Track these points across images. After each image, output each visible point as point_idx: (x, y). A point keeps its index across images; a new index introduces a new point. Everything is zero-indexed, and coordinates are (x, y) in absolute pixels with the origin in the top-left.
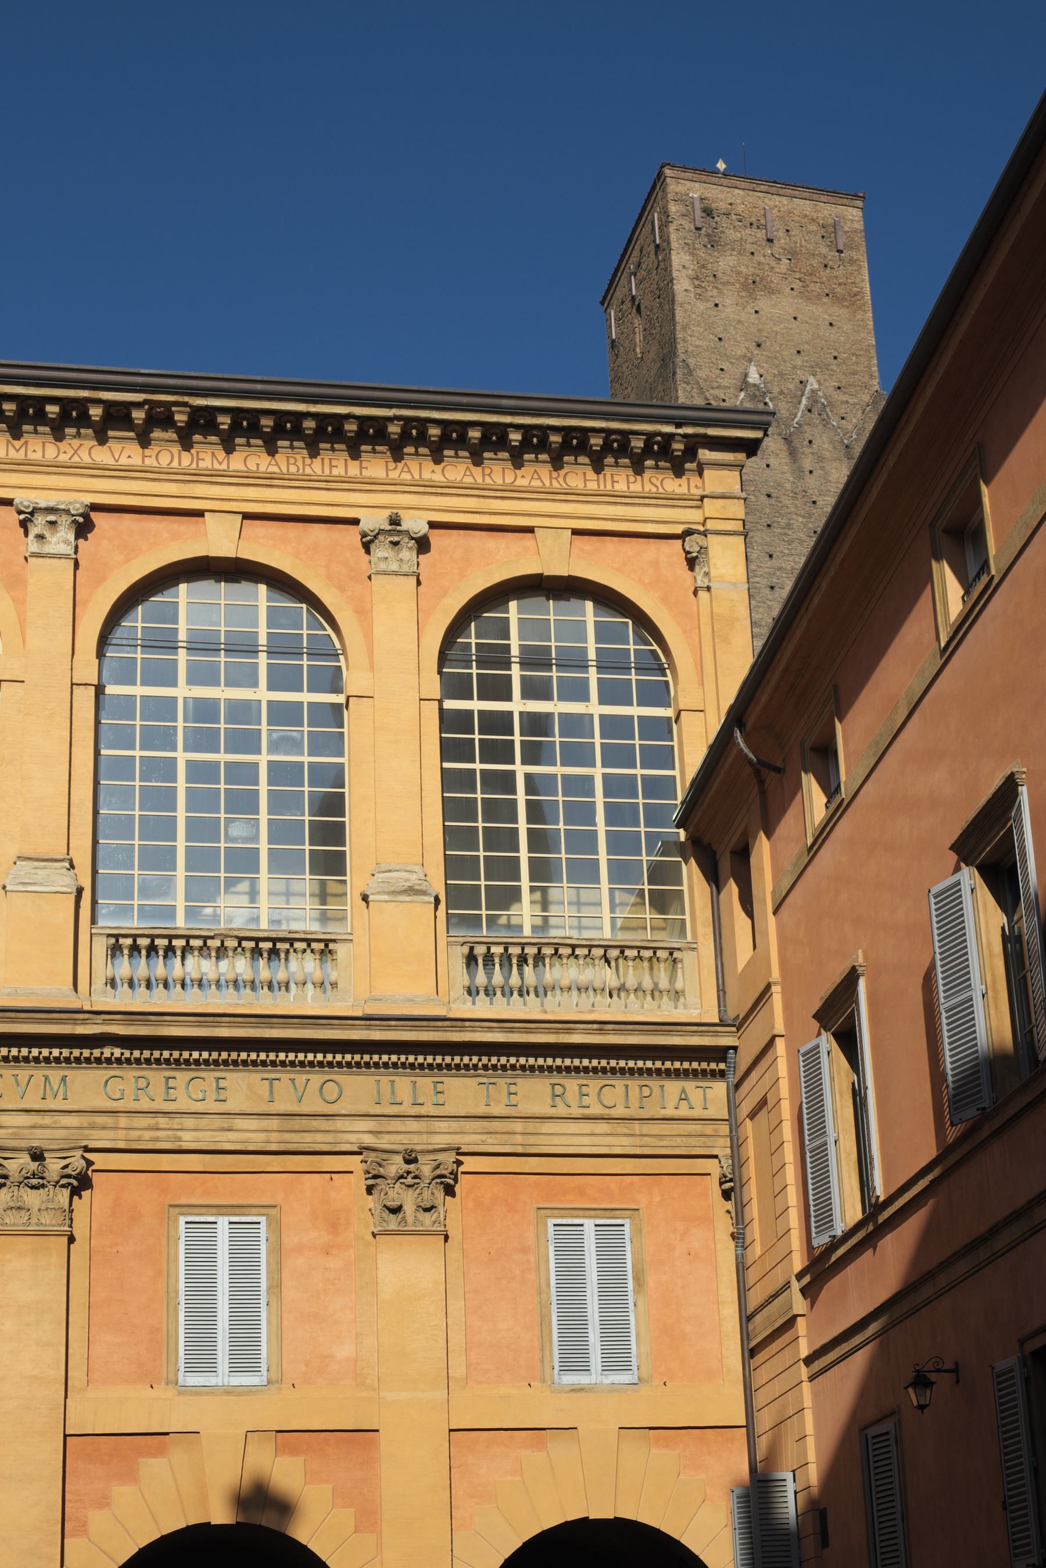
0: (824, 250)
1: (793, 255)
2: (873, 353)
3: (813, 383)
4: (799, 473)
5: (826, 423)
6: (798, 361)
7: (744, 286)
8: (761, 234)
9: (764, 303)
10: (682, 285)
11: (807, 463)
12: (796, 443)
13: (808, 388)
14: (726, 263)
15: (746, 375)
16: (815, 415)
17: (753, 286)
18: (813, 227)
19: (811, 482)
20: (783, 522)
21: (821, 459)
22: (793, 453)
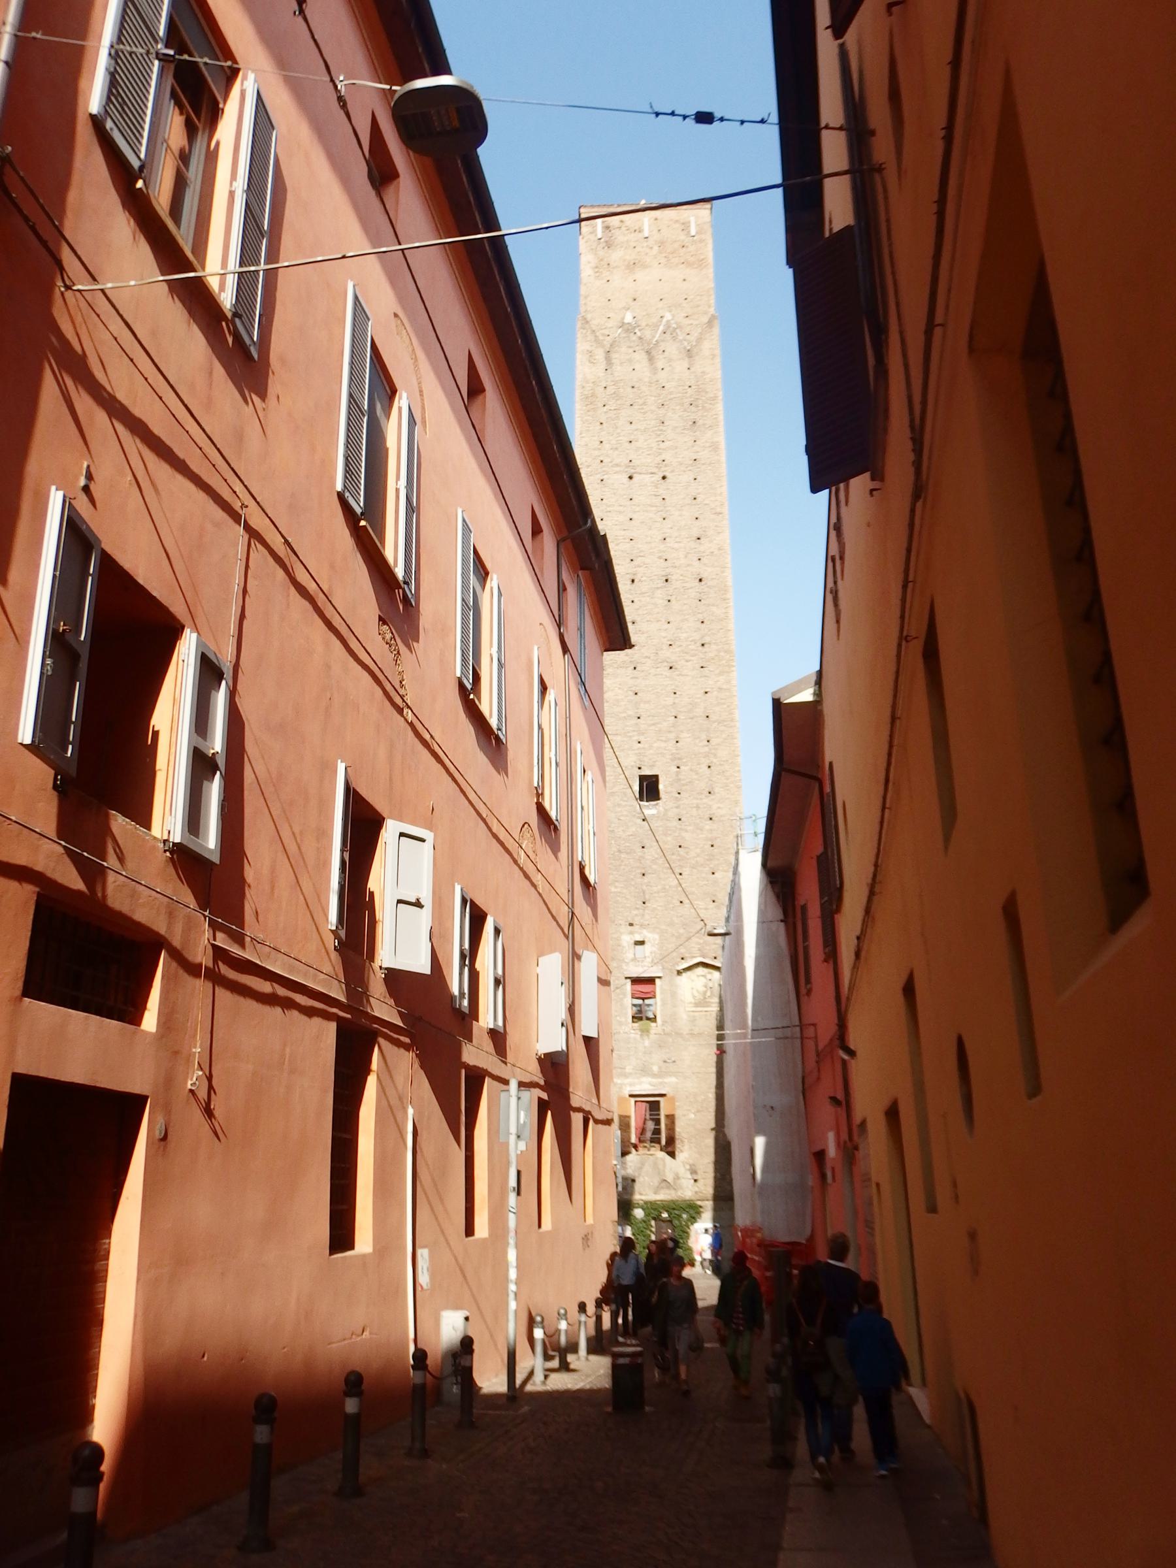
0: (682, 237)
1: (661, 244)
2: (712, 292)
3: (668, 316)
4: (654, 371)
5: (674, 339)
6: (661, 304)
7: (628, 267)
8: (640, 235)
9: (640, 275)
10: (586, 272)
11: (660, 365)
12: (654, 353)
13: (665, 320)
14: (616, 255)
15: (623, 318)
16: (668, 335)
17: (633, 266)
18: (677, 225)
19: (662, 376)
20: (641, 401)
21: (670, 360)
22: (651, 359)
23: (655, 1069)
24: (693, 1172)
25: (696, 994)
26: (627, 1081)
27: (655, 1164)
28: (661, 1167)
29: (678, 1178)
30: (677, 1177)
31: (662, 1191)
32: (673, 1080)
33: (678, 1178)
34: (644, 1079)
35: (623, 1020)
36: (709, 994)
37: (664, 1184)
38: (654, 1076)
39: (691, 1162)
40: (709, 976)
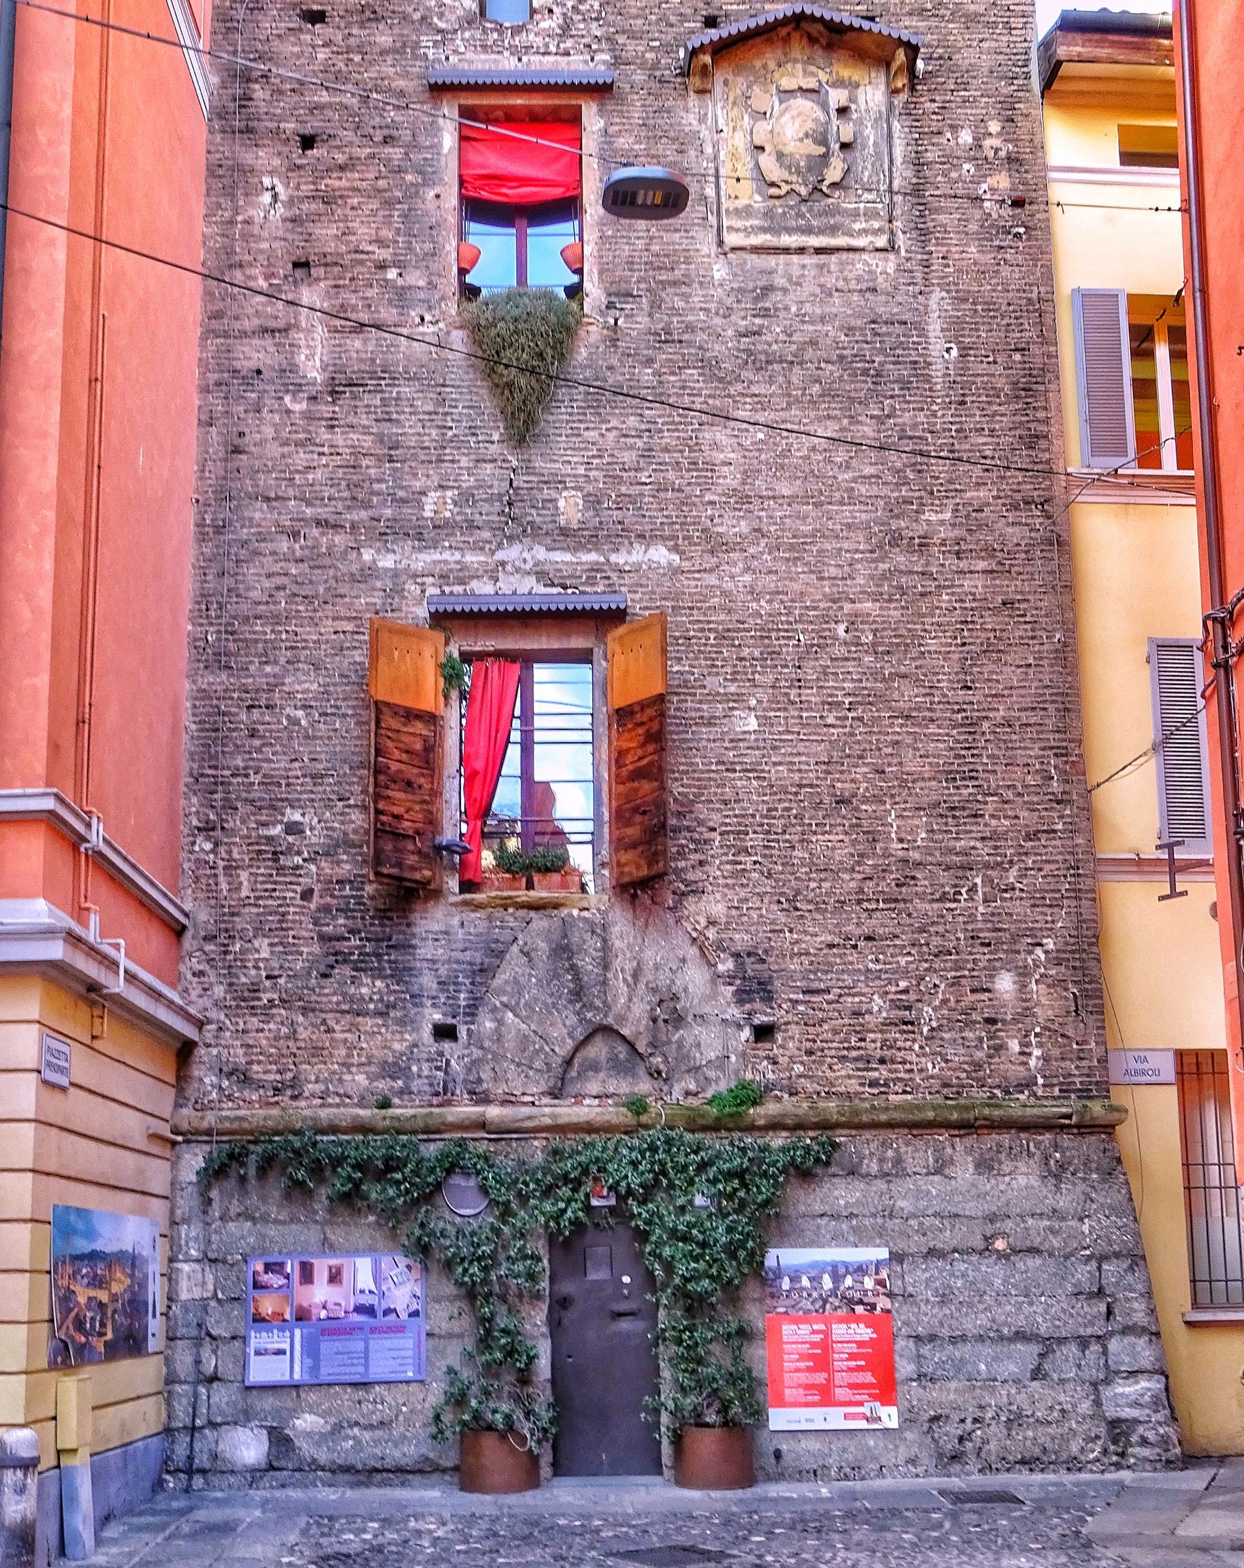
23: (570, 507)
24: (754, 986)
25: (773, 171)
26: (423, 560)
27: (563, 951)
28: (587, 963)
29: (677, 1020)
30: (670, 1012)
31: (594, 1087)
32: (660, 554)
33: (677, 1020)
34: (511, 553)
35: (416, 278)
36: (834, 173)
37: (598, 1050)
38: (565, 536)
39: (741, 940)
40: (837, 97)
